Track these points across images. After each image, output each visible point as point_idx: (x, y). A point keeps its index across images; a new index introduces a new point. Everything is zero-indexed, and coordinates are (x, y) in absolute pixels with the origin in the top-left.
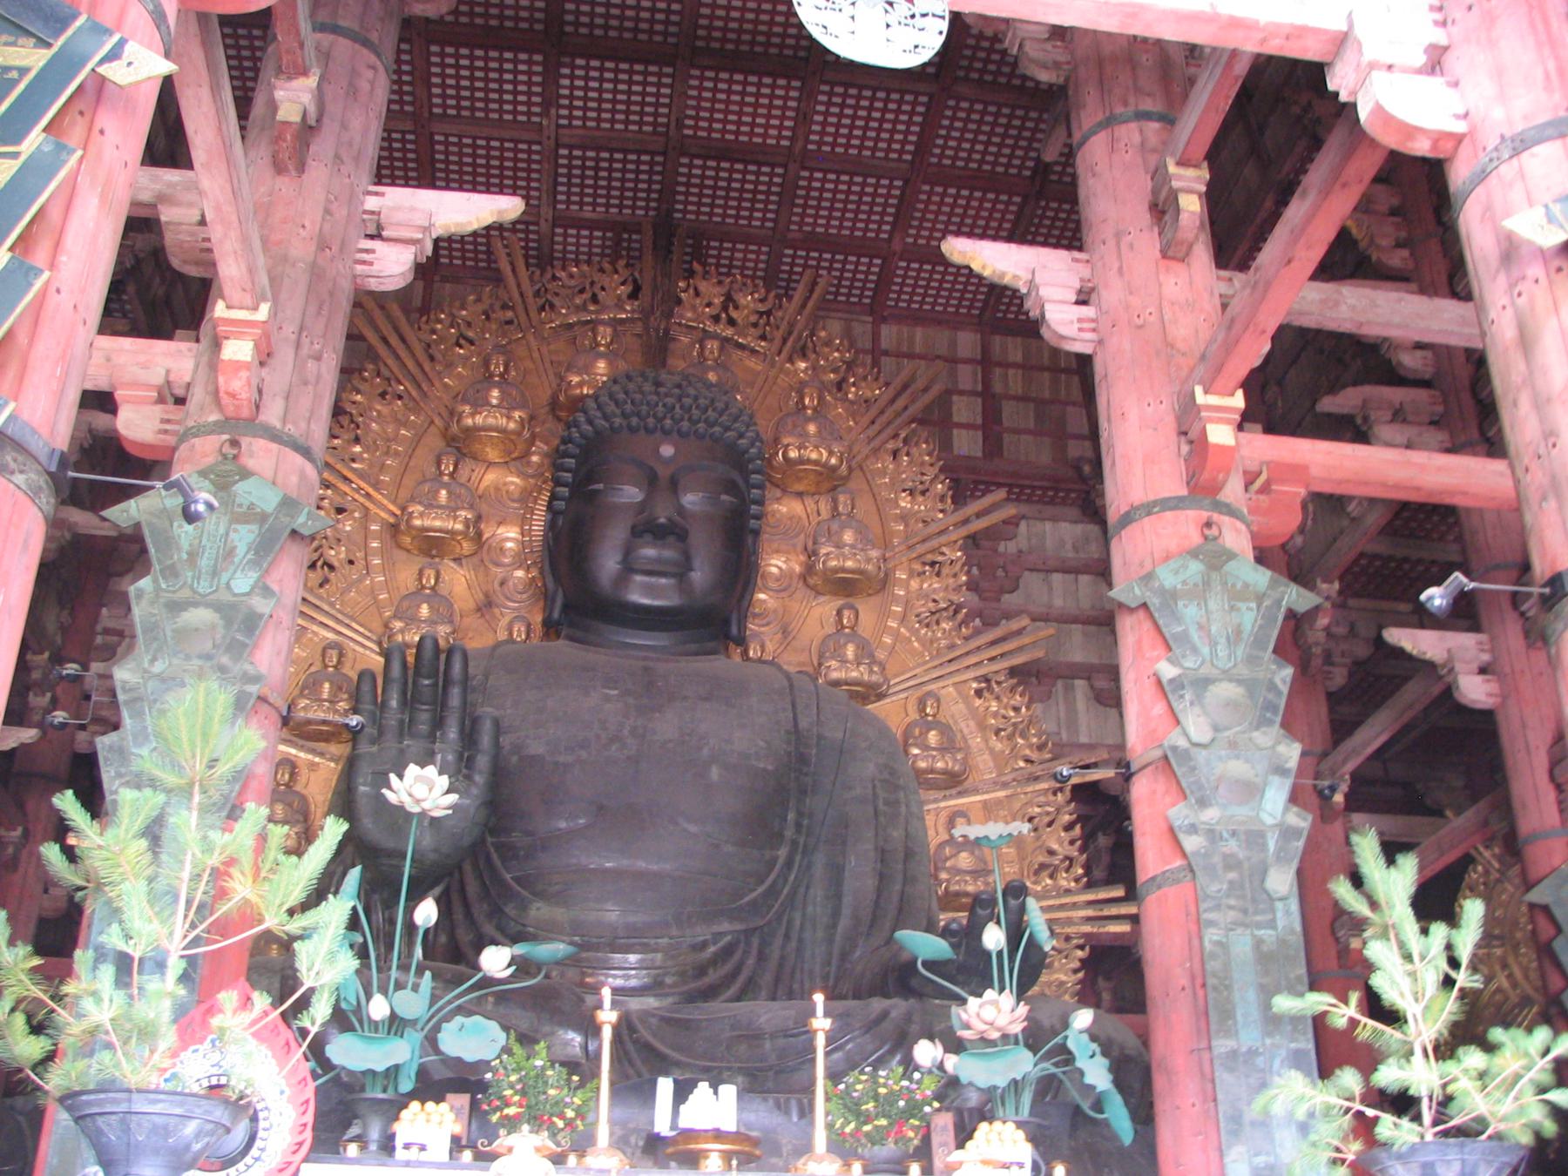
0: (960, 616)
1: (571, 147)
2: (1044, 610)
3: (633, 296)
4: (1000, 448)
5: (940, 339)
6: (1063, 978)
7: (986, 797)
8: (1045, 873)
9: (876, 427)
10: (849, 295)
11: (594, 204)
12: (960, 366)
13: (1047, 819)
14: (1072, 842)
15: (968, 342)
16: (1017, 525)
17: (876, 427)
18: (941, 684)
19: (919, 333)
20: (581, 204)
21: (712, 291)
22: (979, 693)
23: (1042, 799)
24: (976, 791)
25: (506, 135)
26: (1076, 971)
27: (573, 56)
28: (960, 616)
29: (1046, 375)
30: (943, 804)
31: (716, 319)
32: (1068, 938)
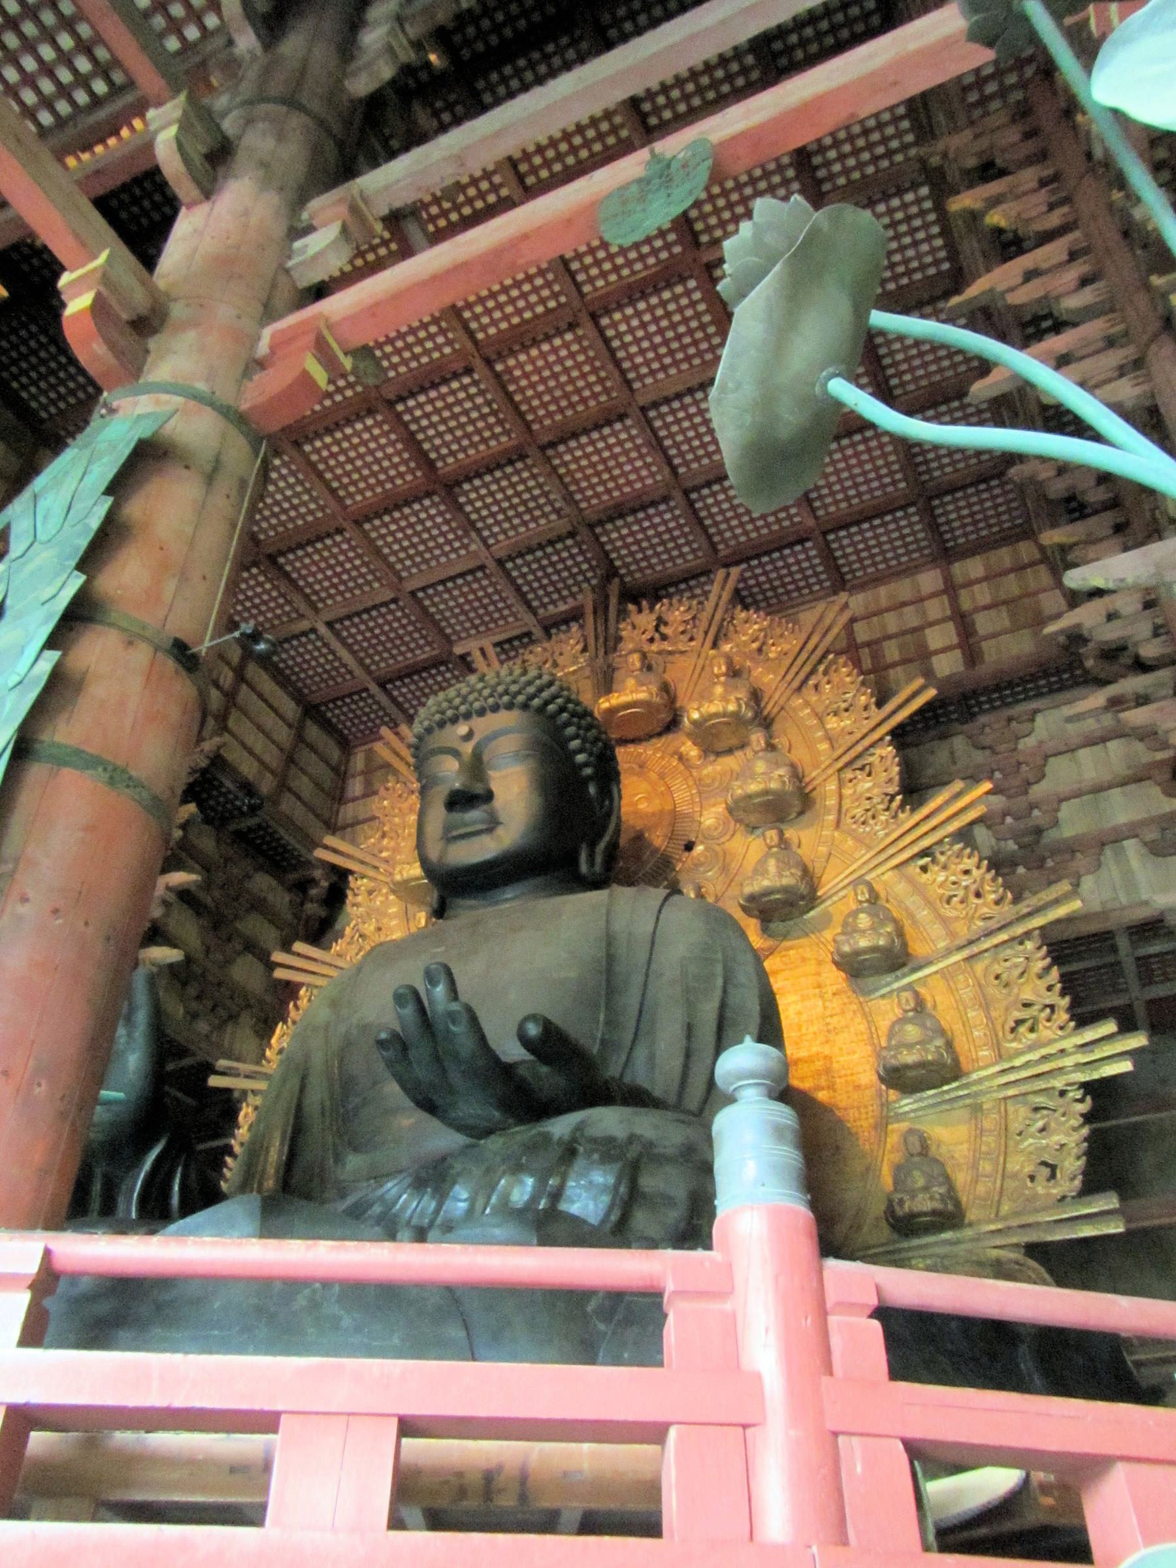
0: (895, 804)
1: (511, 558)
2: (1076, 786)
3: (585, 650)
4: (980, 654)
5: (903, 589)
6: (1063, 1139)
7: (941, 965)
8: (1022, 1029)
9: (794, 670)
10: (809, 586)
11: (563, 598)
12: (927, 603)
13: (1017, 972)
14: (1050, 988)
15: (930, 580)
16: (1033, 720)
17: (794, 670)
18: (879, 871)
19: (883, 591)
20: (553, 602)
21: (645, 620)
22: (924, 869)
23: (1009, 952)
24: (929, 963)
25: (459, 569)
26: (1075, 1129)
27: (459, 484)
28: (895, 804)
29: (1012, 576)
30: (896, 985)
31: (652, 640)
32: (1063, 1093)
